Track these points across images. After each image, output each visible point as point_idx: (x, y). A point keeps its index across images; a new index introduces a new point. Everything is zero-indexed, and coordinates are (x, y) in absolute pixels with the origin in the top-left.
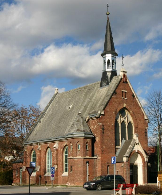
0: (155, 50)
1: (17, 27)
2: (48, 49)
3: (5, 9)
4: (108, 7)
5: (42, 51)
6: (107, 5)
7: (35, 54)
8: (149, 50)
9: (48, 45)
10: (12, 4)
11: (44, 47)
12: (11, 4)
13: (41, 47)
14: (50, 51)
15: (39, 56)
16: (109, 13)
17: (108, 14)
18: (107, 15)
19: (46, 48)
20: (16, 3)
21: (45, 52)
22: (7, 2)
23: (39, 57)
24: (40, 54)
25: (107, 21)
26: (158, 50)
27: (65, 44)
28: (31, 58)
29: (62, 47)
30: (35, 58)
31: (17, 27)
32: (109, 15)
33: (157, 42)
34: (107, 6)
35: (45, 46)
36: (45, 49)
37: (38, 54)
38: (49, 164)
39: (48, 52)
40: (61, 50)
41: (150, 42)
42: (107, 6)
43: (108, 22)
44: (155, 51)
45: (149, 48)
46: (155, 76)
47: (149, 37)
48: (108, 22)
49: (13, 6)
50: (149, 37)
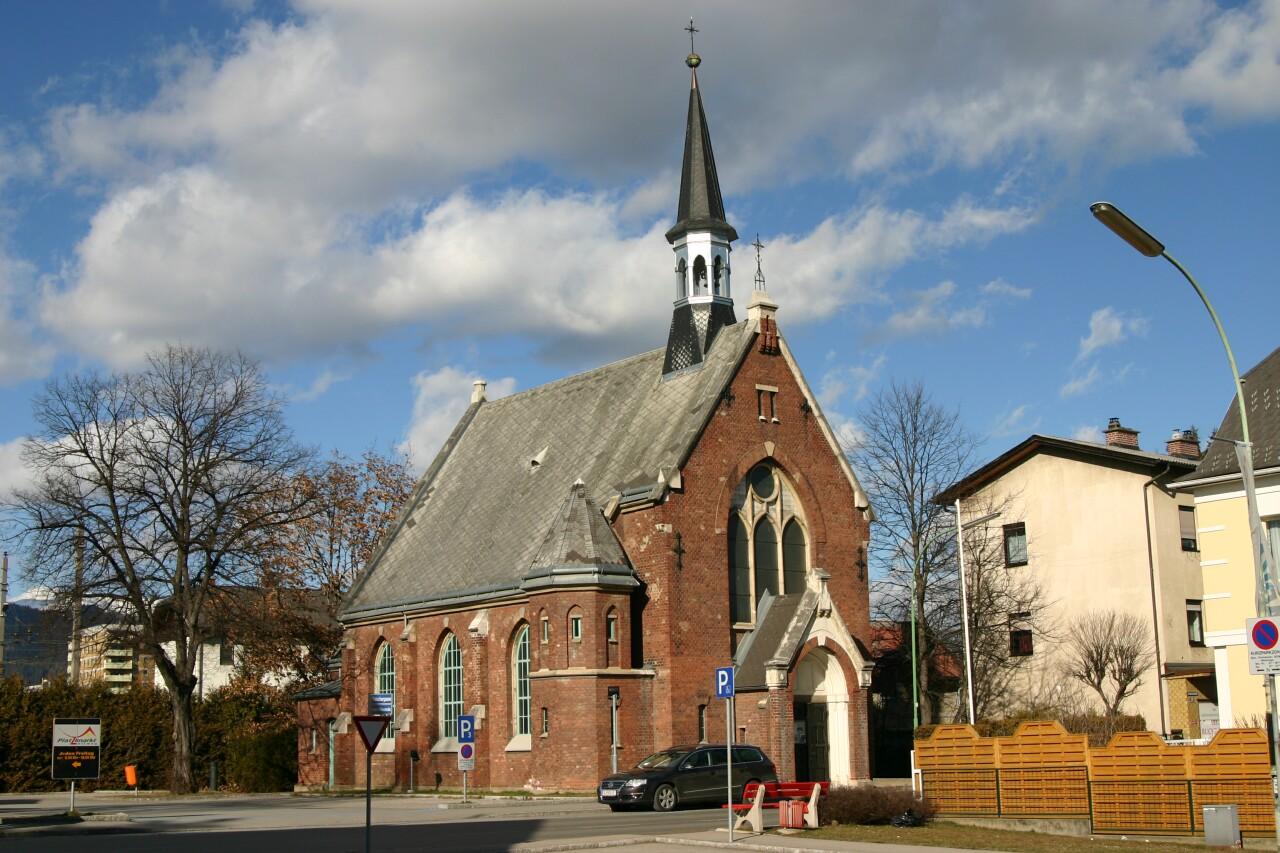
0: (897, 214)
1: (309, 121)
2: (439, 214)
3: (255, 46)
4: (695, 34)
5: (418, 224)
6: (688, 25)
7: (388, 235)
8: (871, 213)
9: (440, 198)
10: (288, 27)
11: (425, 207)
12: (284, 25)
13: (413, 206)
14: (448, 221)
15: (404, 242)
16: (700, 60)
17: (694, 61)
18: (691, 66)
19: (431, 209)
20: (302, 21)
21: (426, 229)
22: (266, 18)
23: (404, 249)
24: (406, 235)
25: (692, 90)
26: (909, 211)
27: (511, 193)
28: (370, 253)
29: (500, 203)
30: (386, 254)
31: (309, 121)
32: (697, 65)
33: (903, 179)
34: (692, 30)
35: (429, 204)
36: (427, 213)
37: (398, 236)
38: (450, 666)
39: (441, 226)
40: (496, 219)
41: (872, 180)
42: (692, 30)
43: (695, 97)
44: (894, 217)
45: (871, 206)
46: (898, 321)
47: (872, 156)
48: (695, 97)
49: (289, 32)
50: (872, 156)
